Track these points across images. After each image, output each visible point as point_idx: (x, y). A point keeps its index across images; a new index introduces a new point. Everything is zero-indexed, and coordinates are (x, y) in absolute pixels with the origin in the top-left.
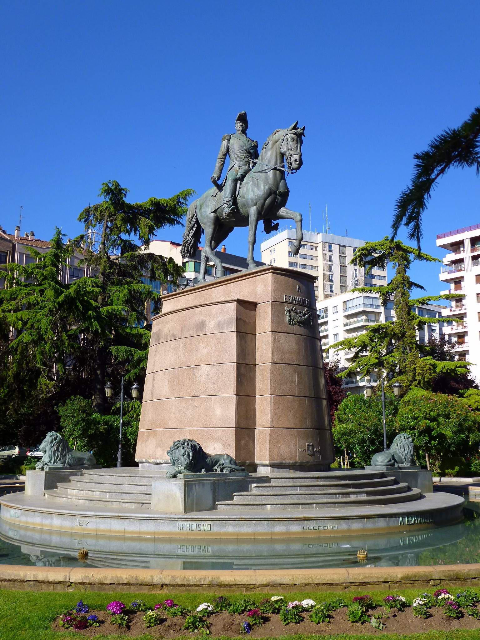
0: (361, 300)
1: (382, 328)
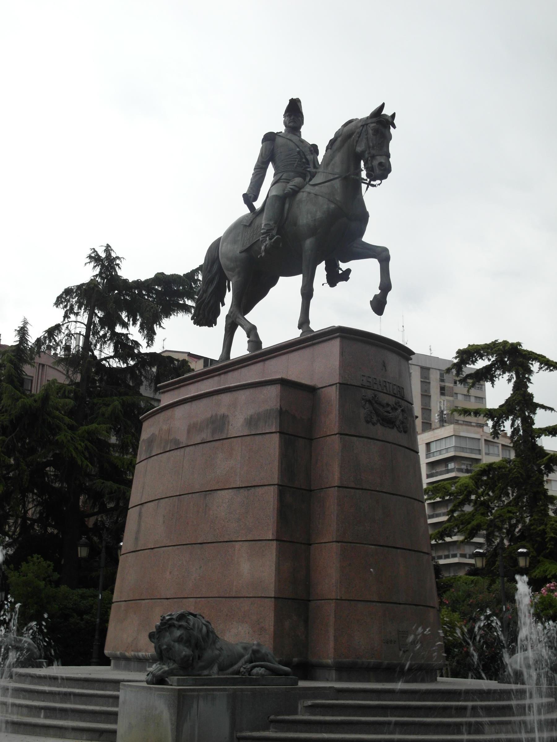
0: (453, 442)
1: (495, 469)
